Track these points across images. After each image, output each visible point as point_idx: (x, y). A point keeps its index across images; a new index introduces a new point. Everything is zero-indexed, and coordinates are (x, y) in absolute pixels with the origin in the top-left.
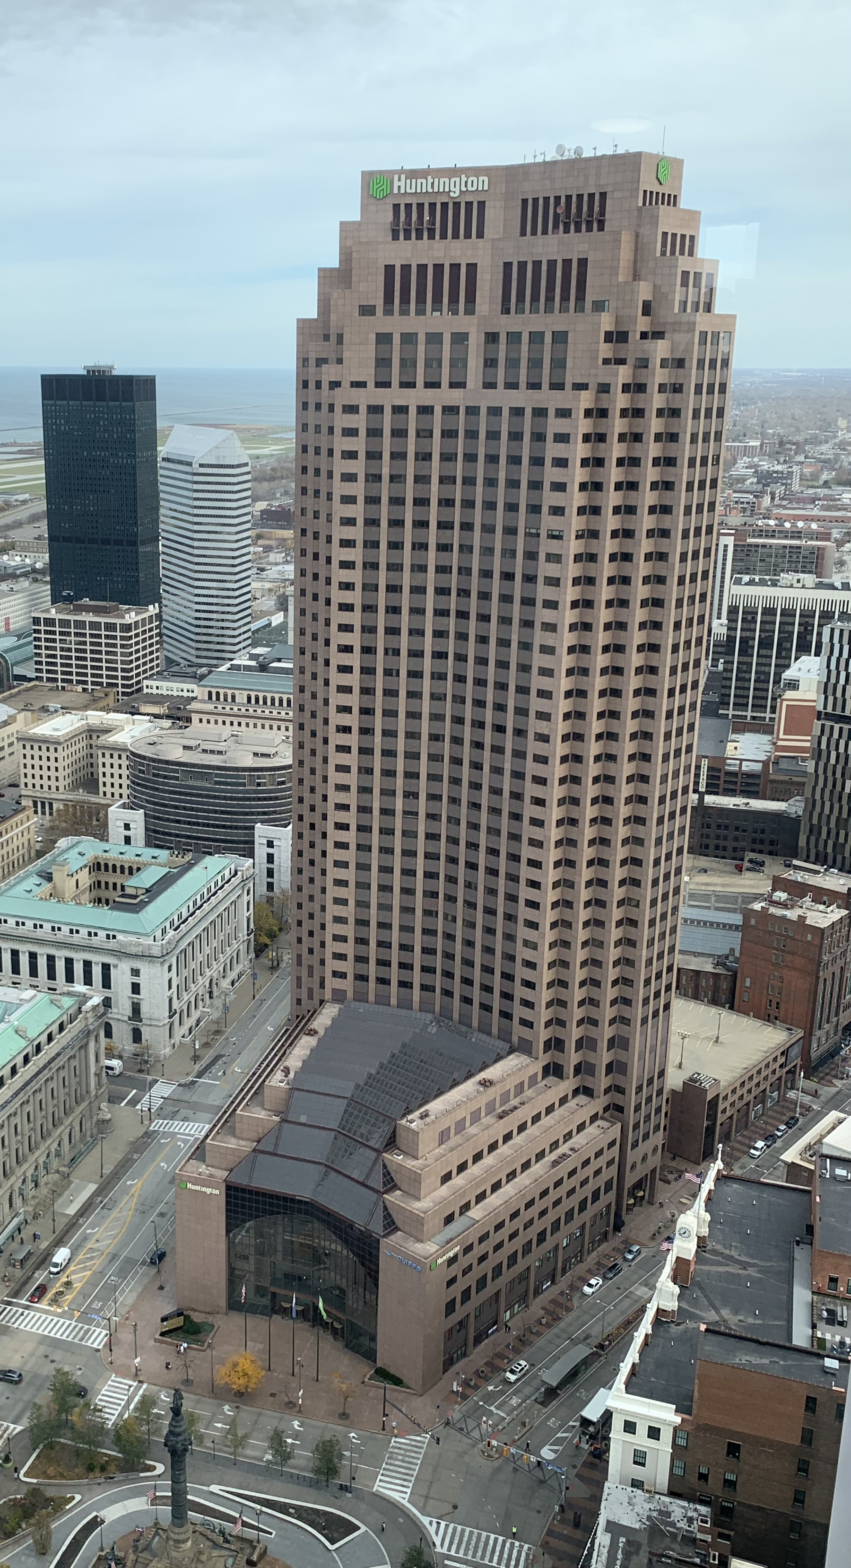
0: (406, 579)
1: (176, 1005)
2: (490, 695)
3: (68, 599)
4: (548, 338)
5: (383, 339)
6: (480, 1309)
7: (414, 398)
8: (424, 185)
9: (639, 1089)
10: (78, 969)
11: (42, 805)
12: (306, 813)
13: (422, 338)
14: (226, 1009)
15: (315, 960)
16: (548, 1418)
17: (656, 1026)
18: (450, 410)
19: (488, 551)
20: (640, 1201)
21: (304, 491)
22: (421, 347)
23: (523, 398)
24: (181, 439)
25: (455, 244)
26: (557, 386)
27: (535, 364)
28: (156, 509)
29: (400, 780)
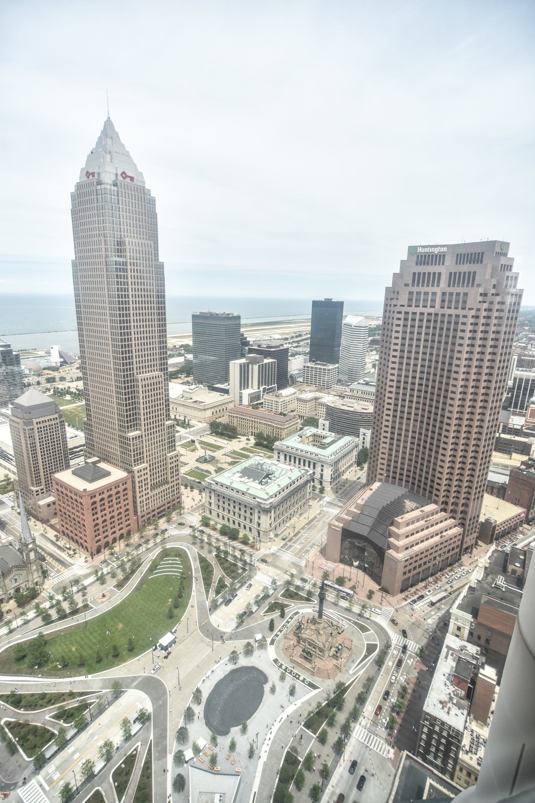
1: (333, 476)
3: (313, 361)
4: (462, 295)
5: (411, 293)
6: (413, 576)
7: (420, 310)
8: (427, 250)
9: (470, 520)
11: (301, 417)
12: (376, 427)
13: (422, 293)
15: (374, 469)
16: (431, 611)
17: (478, 502)
18: (429, 314)
19: (438, 355)
21: (384, 335)
22: (422, 296)
23: (452, 311)
24: (350, 319)
25: (435, 267)
26: (464, 308)
27: (457, 302)
28: (340, 337)
29: (405, 420)
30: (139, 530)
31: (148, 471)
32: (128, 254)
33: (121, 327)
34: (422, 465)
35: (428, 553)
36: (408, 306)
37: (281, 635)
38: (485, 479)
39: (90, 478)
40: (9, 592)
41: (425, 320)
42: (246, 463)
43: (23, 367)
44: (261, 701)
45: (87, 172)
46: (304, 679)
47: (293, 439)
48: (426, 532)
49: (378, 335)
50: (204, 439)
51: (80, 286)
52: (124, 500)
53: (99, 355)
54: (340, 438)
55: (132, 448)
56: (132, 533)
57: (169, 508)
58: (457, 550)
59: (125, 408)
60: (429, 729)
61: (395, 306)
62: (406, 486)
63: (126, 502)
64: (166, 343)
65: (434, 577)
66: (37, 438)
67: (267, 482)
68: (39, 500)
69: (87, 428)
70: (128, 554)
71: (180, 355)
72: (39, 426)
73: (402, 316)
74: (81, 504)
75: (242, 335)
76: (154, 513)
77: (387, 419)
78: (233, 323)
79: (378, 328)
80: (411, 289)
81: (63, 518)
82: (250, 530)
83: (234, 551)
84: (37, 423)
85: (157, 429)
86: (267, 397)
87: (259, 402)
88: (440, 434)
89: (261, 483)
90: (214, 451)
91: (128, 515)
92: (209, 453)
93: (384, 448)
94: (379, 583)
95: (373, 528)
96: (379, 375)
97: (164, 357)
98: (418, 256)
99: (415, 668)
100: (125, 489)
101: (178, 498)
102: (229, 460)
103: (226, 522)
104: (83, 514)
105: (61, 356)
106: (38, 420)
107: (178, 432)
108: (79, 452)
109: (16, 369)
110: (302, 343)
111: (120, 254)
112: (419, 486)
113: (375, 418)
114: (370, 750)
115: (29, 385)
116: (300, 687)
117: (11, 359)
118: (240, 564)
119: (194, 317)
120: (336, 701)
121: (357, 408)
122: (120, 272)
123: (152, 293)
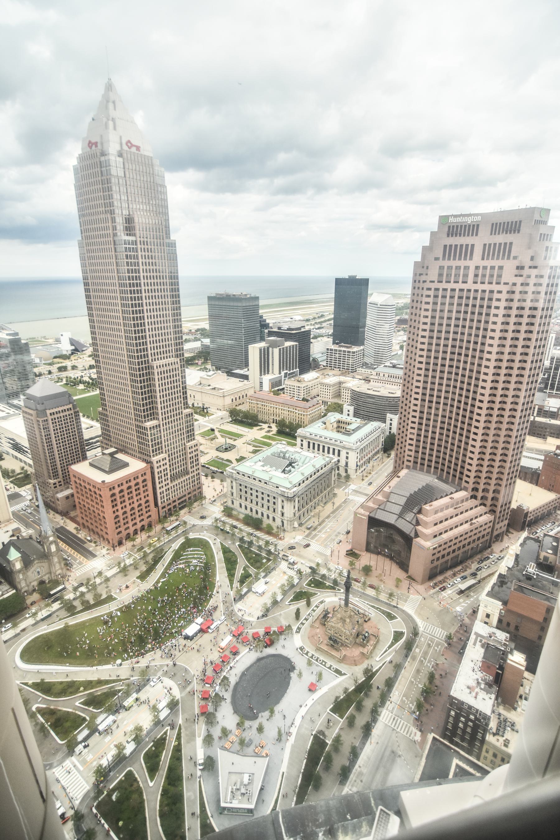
0: (442, 342)
1: (359, 464)
2: (466, 380)
5: (441, 268)
6: (442, 564)
8: (459, 220)
9: (502, 506)
10: (331, 450)
11: (324, 403)
12: (403, 412)
13: (454, 268)
14: (373, 467)
17: (510, 488)
18: (461, 290)
20: (497, 540)
21: (412, 314)
22: (454, 271)
23: (486, 287)
24: (376, 297)
26: (498, 283)
29: (434, 404)
30: (160, 521)
31: (167, 461)
32: (137, 232)
33: (133, 311)
34: (452, 450)
35: (457, 541)
36: (439, 282)
37: (307, 623)
38: (518, 465)
39: (107, 470)
40: (32, 584)
41: (456, 297)
42: (267, 452)
43: (33, 356)
44: (287, 688)
45: (90, 142)
46: (331, 666)
47: (316, 426)
48: (455, 519)
49: (406, 314)
50: (223, 427)
51: (88, 268)
52: (144, 492)
53: (111, 341)
54: (366, 424)
55: (150, 438)
56: (153, 523)
57: (190, 498)
58: (488, 537)
59: (141, 397)
60: (456, 712)
61: (424, 282)
62: (435, 473)
63: (146, 493)
64: (181, 327)
65: (464, 565)
66: (52, 429)
67: (290, 471)
68: (57, 493)
69: (103, 418)
70: (150, 545)
71: (196, 340)
72: (53, 417)
73: (431, 293)
74: (100, 496)
75: (261, 317)
76: (174, 504)
77: (415, 405)
78: (251, 304)
79: (405, 307)
80: (441, 263)
81: (83, 511)
82: (274, 519)
83: (258, 542)
84: (51, 414)
85: (175, 418)
86: (288, 383)
87: (281, 387)
88: (471, 419)
89: (284, 471)
90: (235, 440)
91: (149, 506)
92: (229, 441)
93: (411, 434)
94: (406, 571)
95: (401, 516)
96: (407, 357)
97: (179, 342)
98: (449, 227)
99: (443, 655)
100: (144, 481)
101: (199, 488)
102: (251, 448)
103: (248, 512)
104: (102, 506)
105: (72, 344)
106: (52, 411)
107: (196, 420)
108: (95, 443)
109: (26, 358)
110: (324, 325)
111: (128, 232)
112: (448, 473)
113: (403, 402)
114: (397, 733)
115: (40, 375)
116: (327, 674)
117: (20, 348)
118: (264, 554)
119: (210, 298)
120: (363, 688)
121: (384, 392)
122: (130, 251)
123: (164, 274)
